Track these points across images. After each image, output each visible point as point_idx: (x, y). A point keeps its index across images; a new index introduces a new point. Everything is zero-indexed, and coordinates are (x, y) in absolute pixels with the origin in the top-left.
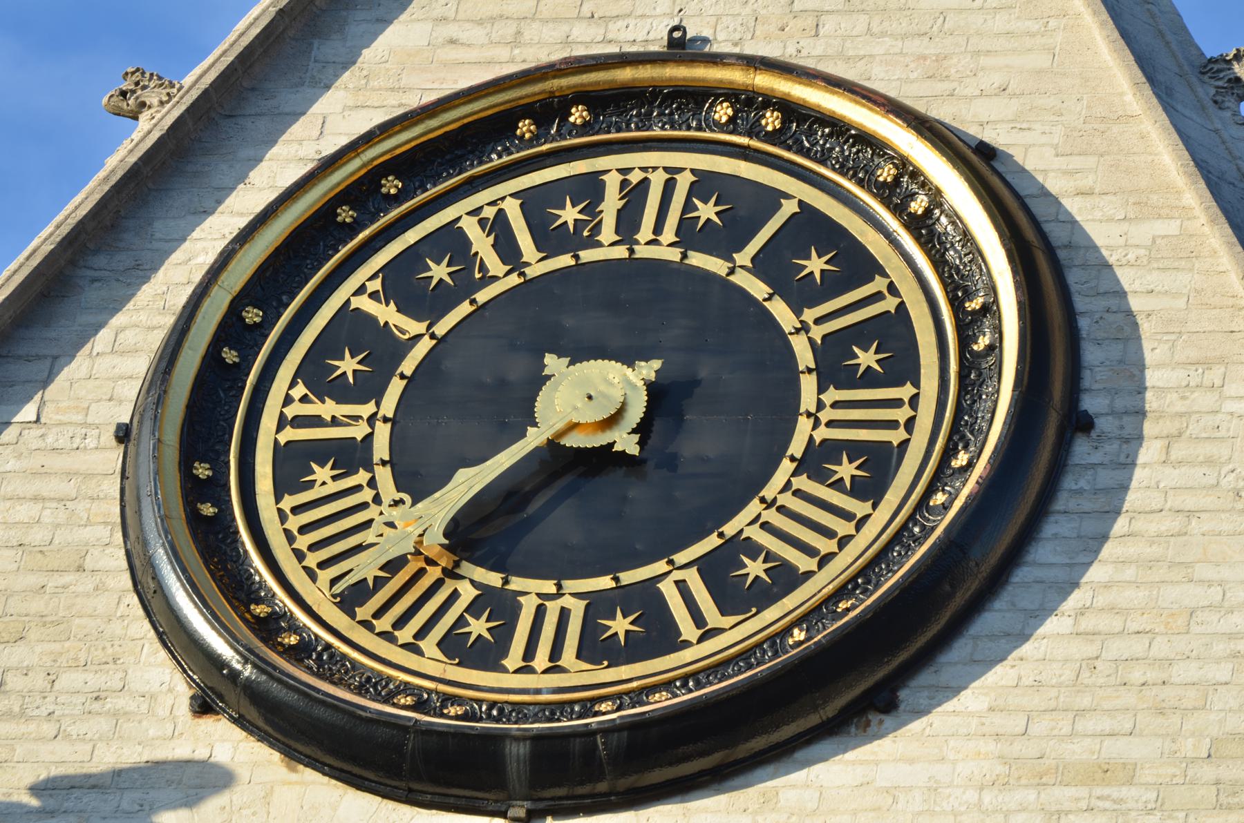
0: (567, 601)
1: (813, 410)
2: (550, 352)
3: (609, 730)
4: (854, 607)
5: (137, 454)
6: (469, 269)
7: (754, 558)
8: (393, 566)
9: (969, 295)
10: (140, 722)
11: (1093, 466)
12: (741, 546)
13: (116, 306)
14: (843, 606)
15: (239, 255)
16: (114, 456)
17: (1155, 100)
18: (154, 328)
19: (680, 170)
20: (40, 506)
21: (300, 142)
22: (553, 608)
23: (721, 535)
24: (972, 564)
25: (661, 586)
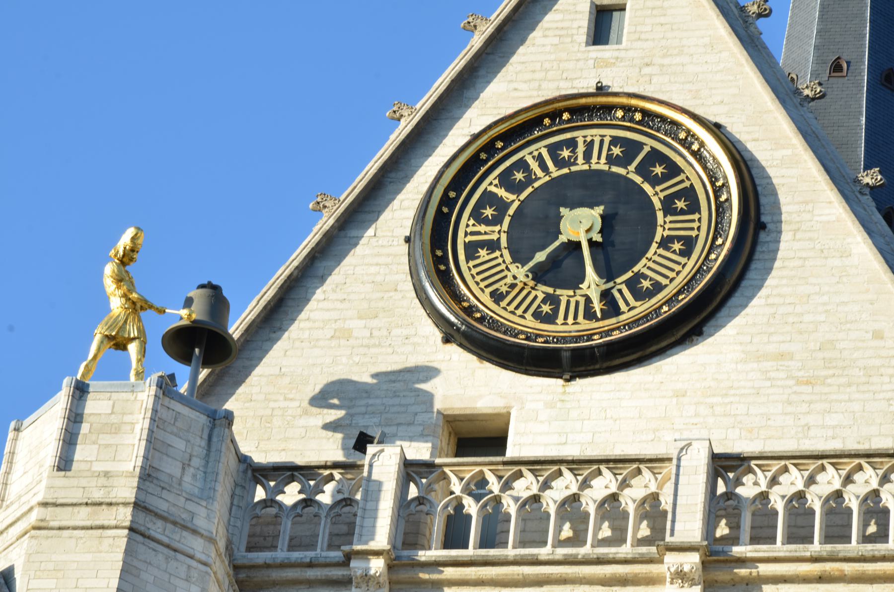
0: (578, 298)
1: (662, 224)
2: (562, 207)
3: (599, 346)
4: (685, 298)
5: (414, 248)
6: (530, 175)
7: (646, 280)
8: (513, 286)
9: (717, 180)
10: (423, 346)
11: (767, 242)
12: (639, 276)
13: (398, 191)
14: (680, 297)
15: (446, 173)
16: (405, 247)
17: (780, 105)
18: (415, 200)
19: (605, 136)
20: (378, 267)
21: (463, 129)
22: (573, 301)
23: (633, 272)
24: (727, 280)
25: (612, 291)
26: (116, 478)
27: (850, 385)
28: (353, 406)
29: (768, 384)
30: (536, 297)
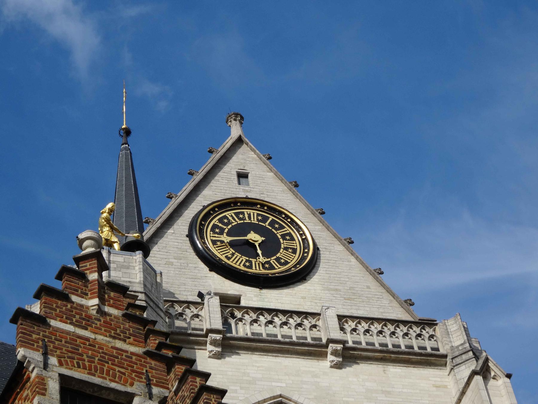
16: (188, 239)
27: (363, 302)
28: (180, 288)
29: (334, 298)
30: (243, 260)
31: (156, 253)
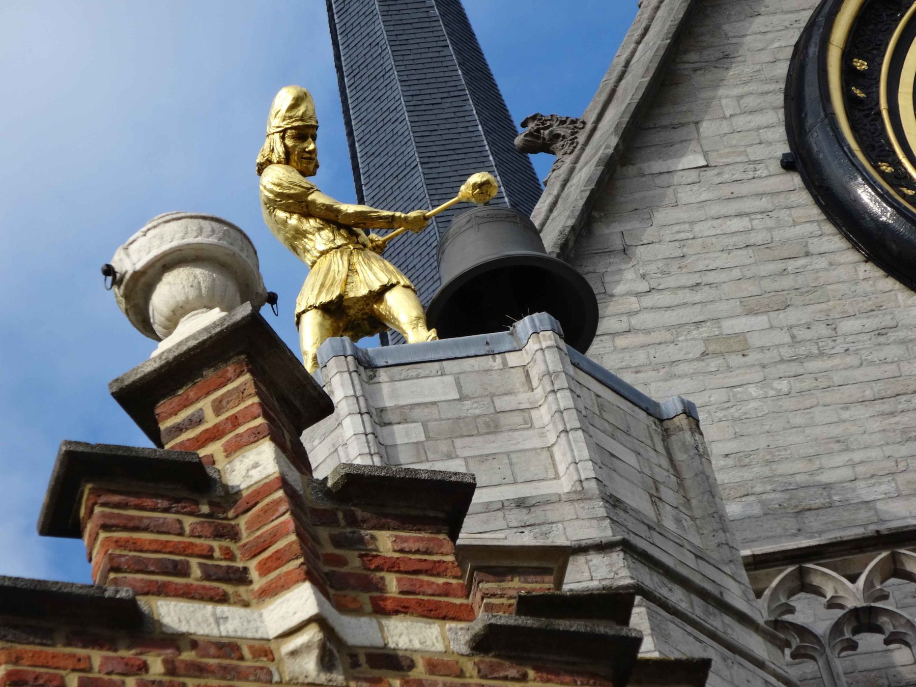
26: (548, 507)
31: (636, 306)
